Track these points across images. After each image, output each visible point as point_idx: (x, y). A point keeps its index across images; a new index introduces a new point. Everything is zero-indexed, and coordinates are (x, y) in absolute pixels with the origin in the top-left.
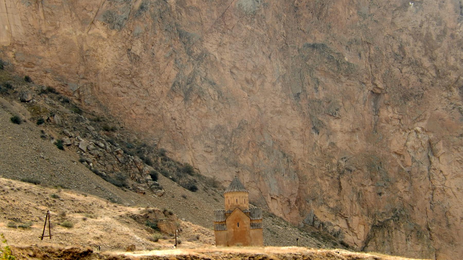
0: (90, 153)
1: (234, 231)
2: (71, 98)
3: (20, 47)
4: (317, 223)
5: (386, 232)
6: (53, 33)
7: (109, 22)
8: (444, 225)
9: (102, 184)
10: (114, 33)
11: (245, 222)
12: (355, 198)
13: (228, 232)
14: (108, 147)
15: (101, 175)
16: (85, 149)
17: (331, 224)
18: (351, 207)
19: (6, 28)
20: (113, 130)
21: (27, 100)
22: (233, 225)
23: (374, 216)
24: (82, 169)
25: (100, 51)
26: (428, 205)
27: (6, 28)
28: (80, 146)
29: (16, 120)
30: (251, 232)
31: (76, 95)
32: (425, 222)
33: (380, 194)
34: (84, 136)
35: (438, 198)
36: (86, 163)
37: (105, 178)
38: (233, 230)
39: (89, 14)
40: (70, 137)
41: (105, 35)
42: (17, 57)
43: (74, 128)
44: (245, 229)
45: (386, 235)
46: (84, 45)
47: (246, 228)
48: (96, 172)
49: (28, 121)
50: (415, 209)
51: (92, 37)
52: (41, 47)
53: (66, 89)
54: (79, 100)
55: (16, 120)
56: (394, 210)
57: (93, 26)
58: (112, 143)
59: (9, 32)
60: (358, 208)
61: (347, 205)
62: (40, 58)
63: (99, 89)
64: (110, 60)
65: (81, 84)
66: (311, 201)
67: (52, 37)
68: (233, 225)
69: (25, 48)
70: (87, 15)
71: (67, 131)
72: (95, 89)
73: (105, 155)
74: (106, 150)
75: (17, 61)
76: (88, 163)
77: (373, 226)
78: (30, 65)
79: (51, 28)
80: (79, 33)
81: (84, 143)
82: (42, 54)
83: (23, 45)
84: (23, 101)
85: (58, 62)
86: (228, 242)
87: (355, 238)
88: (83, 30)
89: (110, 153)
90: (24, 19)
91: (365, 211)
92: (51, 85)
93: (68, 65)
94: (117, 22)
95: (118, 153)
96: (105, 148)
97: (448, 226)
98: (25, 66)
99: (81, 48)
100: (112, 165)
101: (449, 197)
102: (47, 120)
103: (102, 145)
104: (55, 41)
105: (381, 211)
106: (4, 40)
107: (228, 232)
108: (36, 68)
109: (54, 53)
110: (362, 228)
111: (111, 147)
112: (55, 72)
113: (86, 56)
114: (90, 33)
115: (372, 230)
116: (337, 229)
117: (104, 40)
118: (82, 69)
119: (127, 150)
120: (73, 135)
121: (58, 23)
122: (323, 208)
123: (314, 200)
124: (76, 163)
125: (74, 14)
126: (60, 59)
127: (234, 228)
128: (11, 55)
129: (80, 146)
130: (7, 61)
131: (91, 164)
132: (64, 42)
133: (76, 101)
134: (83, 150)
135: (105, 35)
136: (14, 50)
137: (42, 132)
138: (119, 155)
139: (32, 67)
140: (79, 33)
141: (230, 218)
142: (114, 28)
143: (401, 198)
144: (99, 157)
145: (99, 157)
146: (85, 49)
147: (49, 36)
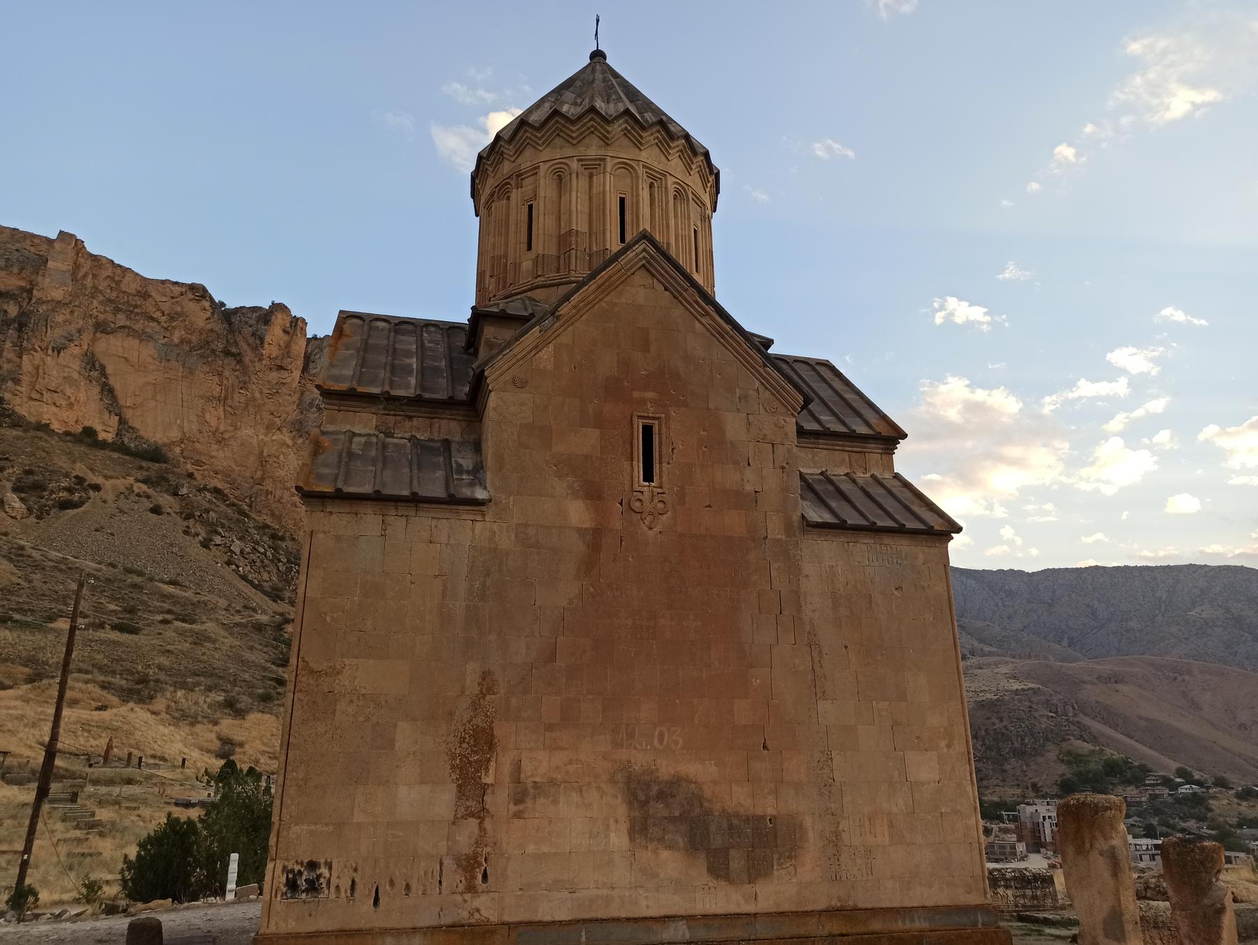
0: (244, 557)
1: (595, 537)
2: (240, 503)
3: (191, 444)
6: (232, 434)
7: (297, 430)
9: (246, 591)
10: (300, 441)
11: (734, 427)
13: (506, 541)
14: (269, 554)
15: (251, 583)
16: (237, 551)
19: (178, 422)
20: (282, 539)
21: (180, 493)
22: (586, 441)
24: (228, 571)
25: (282, 457)
27: (178, 422)
28: (232, 548)
29: (156, 510)
30: (808, 568)
31: (247, 500)
34: (240, 539)
36: (234, 567)
37: (255, 586)
38: (578, 513)
39: (276, 419)
40: (222, 537)
41: (290, 442)
42: (185, 454)
43: (231, 528)
44: (734, 522)
46: (265, 450)
47: (747, 501)
48: (244, 578)
49: (173, 514)
51: (275, 443)
52: (215, 447)
53: (237, 493)
54: (250, 506)
55: (156, 510)
57: (278, 432)
58: (275, 550)
59: (181, 427)
62: (212, 457)
63: (275, 497)
64: (291, 469)
65: (254, 490)
67: (230, 437)
68: (586, 441)
69: (197, 445)
70: (273, 420)
71: (220, 530)
72: (270, 496)
73: (262, 562)
74: (266, 556)
75: (184, 457)
76: (238, 567)
78: (198, 463)
79: (231, 428)
80: (261, 437)
81: (237, 546)
82: (214, 454)
83: (194, 442)
84: (175, 494)
85: (232, 464)
86: (487, 682)
88: (266, 436)
89: (270, 560)
90: (200, 414)
92: (219, 486)
93: (243, 468)
94: (306, 430)
95: (280, 561)
96: (265, 554)
98: (193, 464)
99: (261, 452)
100: (269, 572)
102: (199, 516)
103: (263, 550)
104: (232, 442)
106: (174, 435)
107: (506, 541)
108: (205, 467)
109: (228, 454)
111: (273, 554)
112: (227, 474)
113: (266, 461)
114: (274, 438)
117: (288, 446)
118: (259, 474)
119: (292, 559)
120: (227, 534)
121: (239, 424)
124: (219, 565)
125: (258, 417)
126: (235, 461)
127: (593, 494)
128: (178, 450)
129: (232, 548)
130: (172, 457)
131: (241, 569)
132: (242, 444)
133: (246, 507)
134: (234, 553)
135: (290, 442)
136: (183, 446)
137: (188, 527)
138: (281, 564)
139: (201, 466)
140: (261, 437)
141: (546, 354)
142: (301, 436)
144: (254, 562)
145: (254, 562)
146: (265, 454)
147: (226, 436)
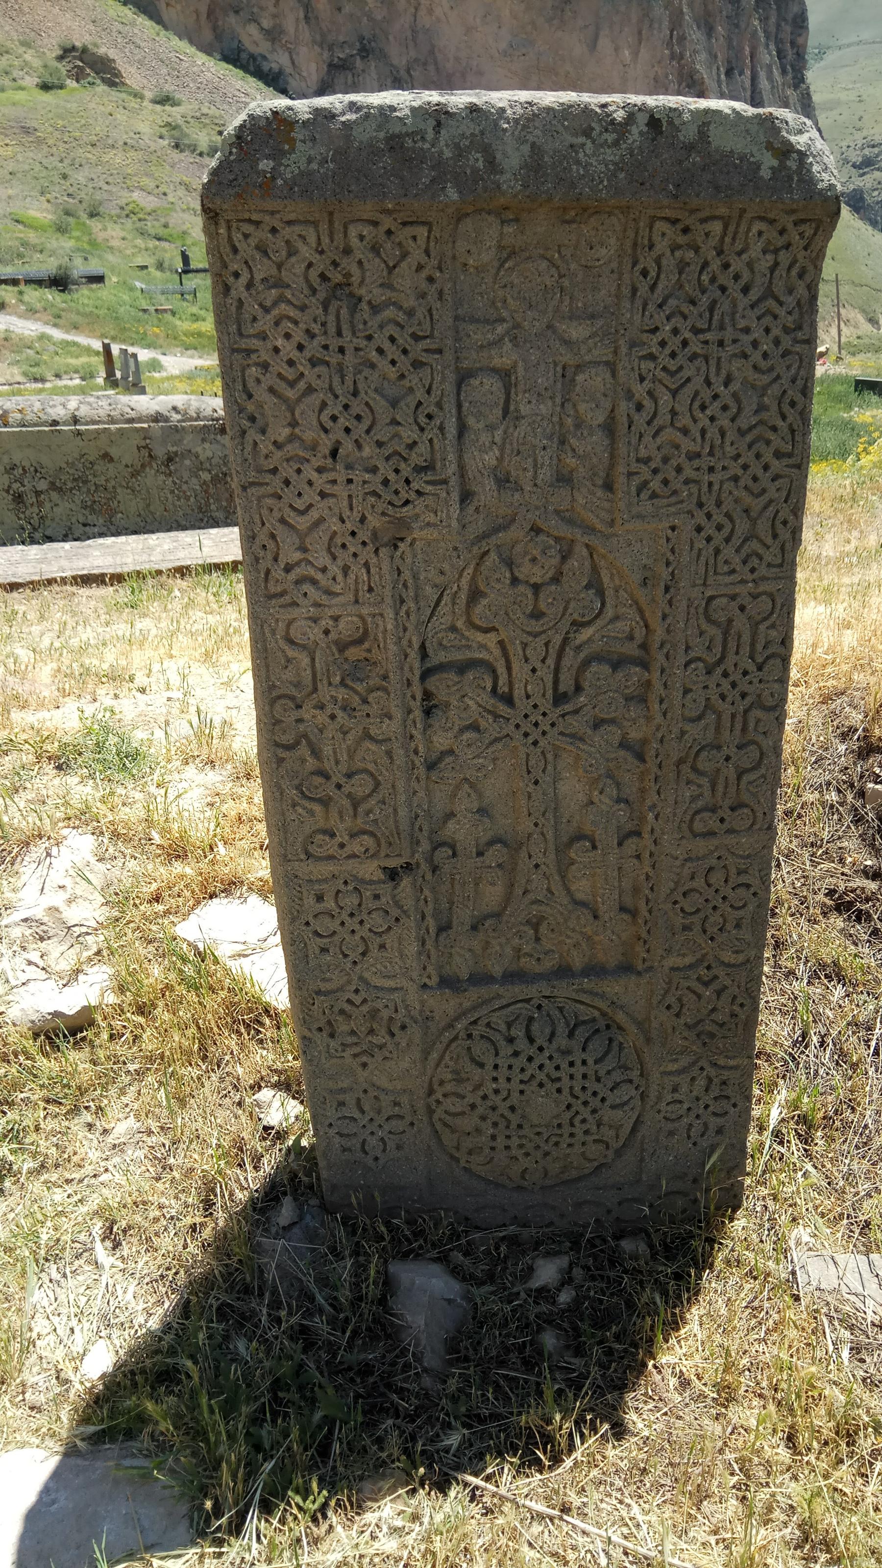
4: (244, 56)
5: (350, 76)
8: (431, 68)
12: (302, 15)
17: (264, 58)
18: (297, 30)
23: (331, 48)
26: (409, 33)
32: (404, 62)
33: (339, 9)
35: (425, 20)
45: (350, 82)
50: (391, 38)
56: (362, 38)
60: (306, 34)
61: (289, 24)
66: (232, 14)
77: (331, 66)
87: (303, 85)
91: (318, 37)
97: (437, 70)
101: (439, 20)
105: (341, 39)
110: (313, 67)
115: (329, 72)
116: (274, 66)
122: (253, 29)
123: (237, 12)
143: (371, 19)
